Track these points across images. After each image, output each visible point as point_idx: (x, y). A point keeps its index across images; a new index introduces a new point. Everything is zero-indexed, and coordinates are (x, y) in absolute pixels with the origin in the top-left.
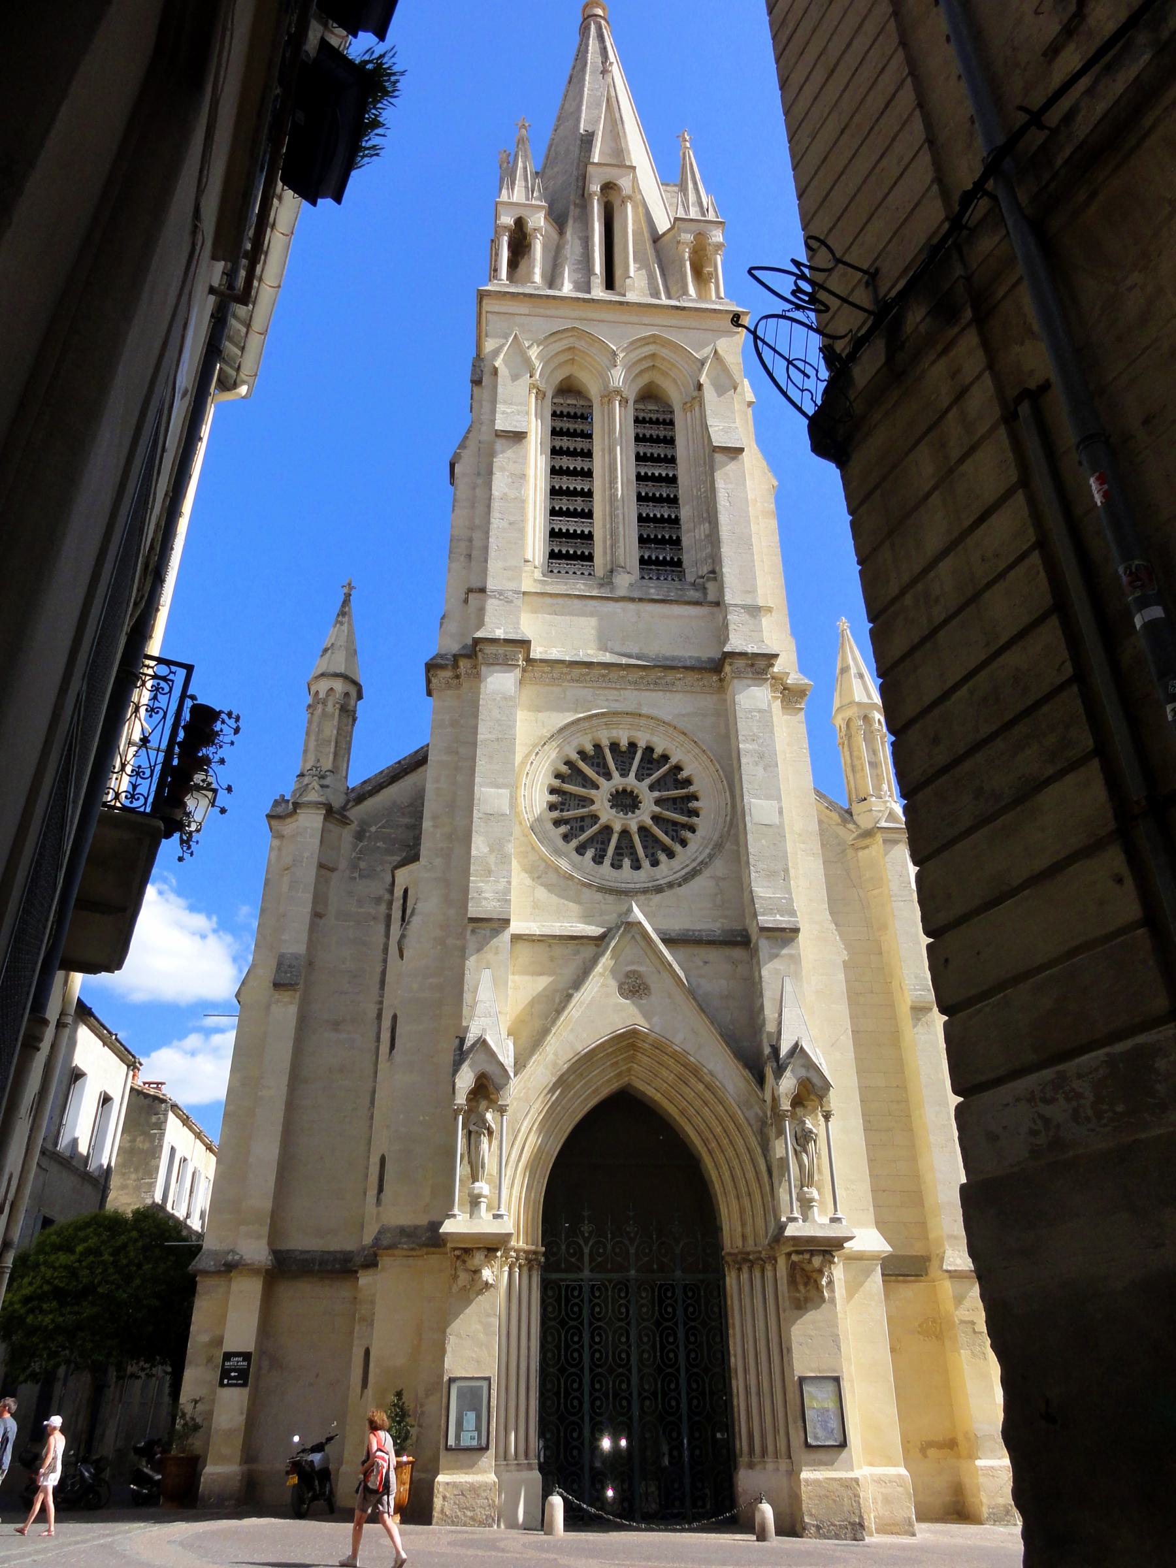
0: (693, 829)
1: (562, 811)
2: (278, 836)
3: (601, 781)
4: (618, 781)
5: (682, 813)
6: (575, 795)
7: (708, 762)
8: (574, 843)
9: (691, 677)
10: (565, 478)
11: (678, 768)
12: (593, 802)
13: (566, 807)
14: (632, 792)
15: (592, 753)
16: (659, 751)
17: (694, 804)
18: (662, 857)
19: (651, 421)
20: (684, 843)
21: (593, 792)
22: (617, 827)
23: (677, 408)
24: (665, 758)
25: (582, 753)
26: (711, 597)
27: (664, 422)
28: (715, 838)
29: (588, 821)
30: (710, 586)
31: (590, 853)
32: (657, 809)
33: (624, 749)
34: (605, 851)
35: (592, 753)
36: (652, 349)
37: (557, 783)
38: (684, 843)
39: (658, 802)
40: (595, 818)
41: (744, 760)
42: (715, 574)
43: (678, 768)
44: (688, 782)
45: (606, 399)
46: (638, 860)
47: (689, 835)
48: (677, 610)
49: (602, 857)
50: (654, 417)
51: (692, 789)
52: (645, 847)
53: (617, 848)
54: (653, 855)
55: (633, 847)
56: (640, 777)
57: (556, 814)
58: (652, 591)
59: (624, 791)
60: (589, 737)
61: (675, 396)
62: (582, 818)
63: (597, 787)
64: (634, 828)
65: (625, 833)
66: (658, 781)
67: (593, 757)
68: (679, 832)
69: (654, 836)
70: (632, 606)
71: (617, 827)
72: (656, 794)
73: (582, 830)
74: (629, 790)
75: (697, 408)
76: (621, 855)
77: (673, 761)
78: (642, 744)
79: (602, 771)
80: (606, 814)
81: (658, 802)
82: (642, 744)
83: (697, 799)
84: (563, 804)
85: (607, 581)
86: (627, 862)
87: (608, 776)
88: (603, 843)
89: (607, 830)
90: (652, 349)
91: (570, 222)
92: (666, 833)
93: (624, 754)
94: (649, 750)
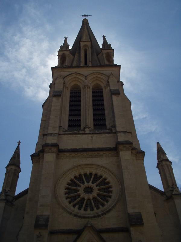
0: (110, 197)
5: (107, 193)
8: (72, 204)
9: (107, 153)
11: (105, 179)
12: (79, 191)
14: (91, 187)
16: (99, 174)
18: (101, 206)
19: (97, 92)
20: (107, 201)
21: (79, 188)
22: (86, 198)
23: (103, 88)
24: (101, 177)
26: (114, 131)
27: (100, 92)
30: (113, 129)
33: (88, 175)
34: (82, 206)
35: (78, 177)
36: (96, 75)
39: (99, 190)
40: (79, 196)
42: (114, 126)
43: (105, 179)
44: (108, 183)
47: (109, 199)
48: (103, 135)
50: (97, 91)
51: (110, 185)
52: (95, 204)
54: (98, 206)
55: (91, 204)
58: (96, 131)
59: (88, 187)
61: (102, 85)
62: (75, 196)
64: (91, 198)
68: (105, 198)
70: (90, 135)
71: (86, 198)
74: (90, 186)
77: (103, 177)
78: (94, 173)
80: (83, 194)
81: (99, 190)
82: (94, 173)
83: (111, 188)
85: (84, 130)
87: (83, 183)
90: (96, 75)
91: (76, 54)
92: (102, 199)
93: (88, 177)
94: (96, 175)
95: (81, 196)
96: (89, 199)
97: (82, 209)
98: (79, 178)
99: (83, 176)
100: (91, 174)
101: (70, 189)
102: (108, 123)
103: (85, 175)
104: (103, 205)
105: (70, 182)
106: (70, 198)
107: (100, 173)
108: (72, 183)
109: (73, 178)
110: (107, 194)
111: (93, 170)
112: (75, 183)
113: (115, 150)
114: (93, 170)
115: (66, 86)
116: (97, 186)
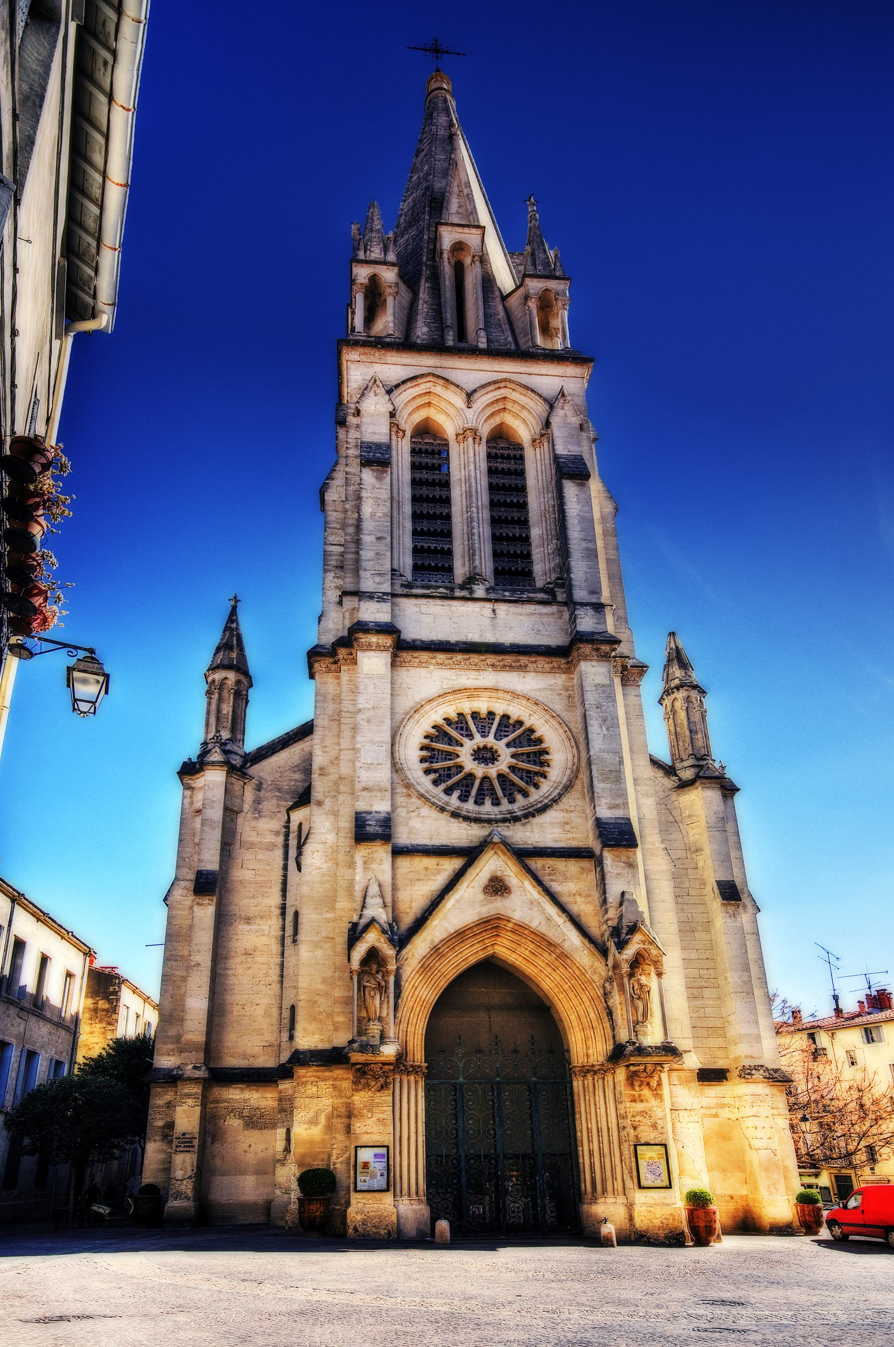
1: (431, 762)
2: (188, 787)
3: (465, 740)
4: (479, 741)
5: (535, 764)
6: (442, 751)
7: (557, 726)
12: (458, 756)
13: (435, 760)
14: (492, 748)
15: (456, 719)
17: (547, 757)
25: (447, 720)
28: (564, 782)
29: (454, 770)
31: (456, 794)
32: (514, 761)
34: (469, 792)
35: (456, 719)
37: (427, 741)
39: (514, 756)
46: (497, 799)
47: (542, 780)
49: (467, 797)
52: (503, 789)
53: (479, 789)
54: (510, 795)
55: (493, 789)
56: (498, 737)
59: (485, 748)
60: (454, 707)
62: (449, 768)
63: (462, 745)
66: (514, 740)
67: (457, 723)
68: (532, 779)
69: (510, 781)
72: (513, 750)
73: (449, 777)
76: (484, 795)
79: (464, 733)
84: (431, 757)
87: (470, 736)
88: (467, 786)
89: (471, 776)
92: (521, 779)
93: (484, 721)
97: (471, 800)
98: (460, 722)
101: (433, 750)
106: (436, 771)
108: (439, 734)
110: (536, 768)
112: (446, 734)
116: (508, 745)
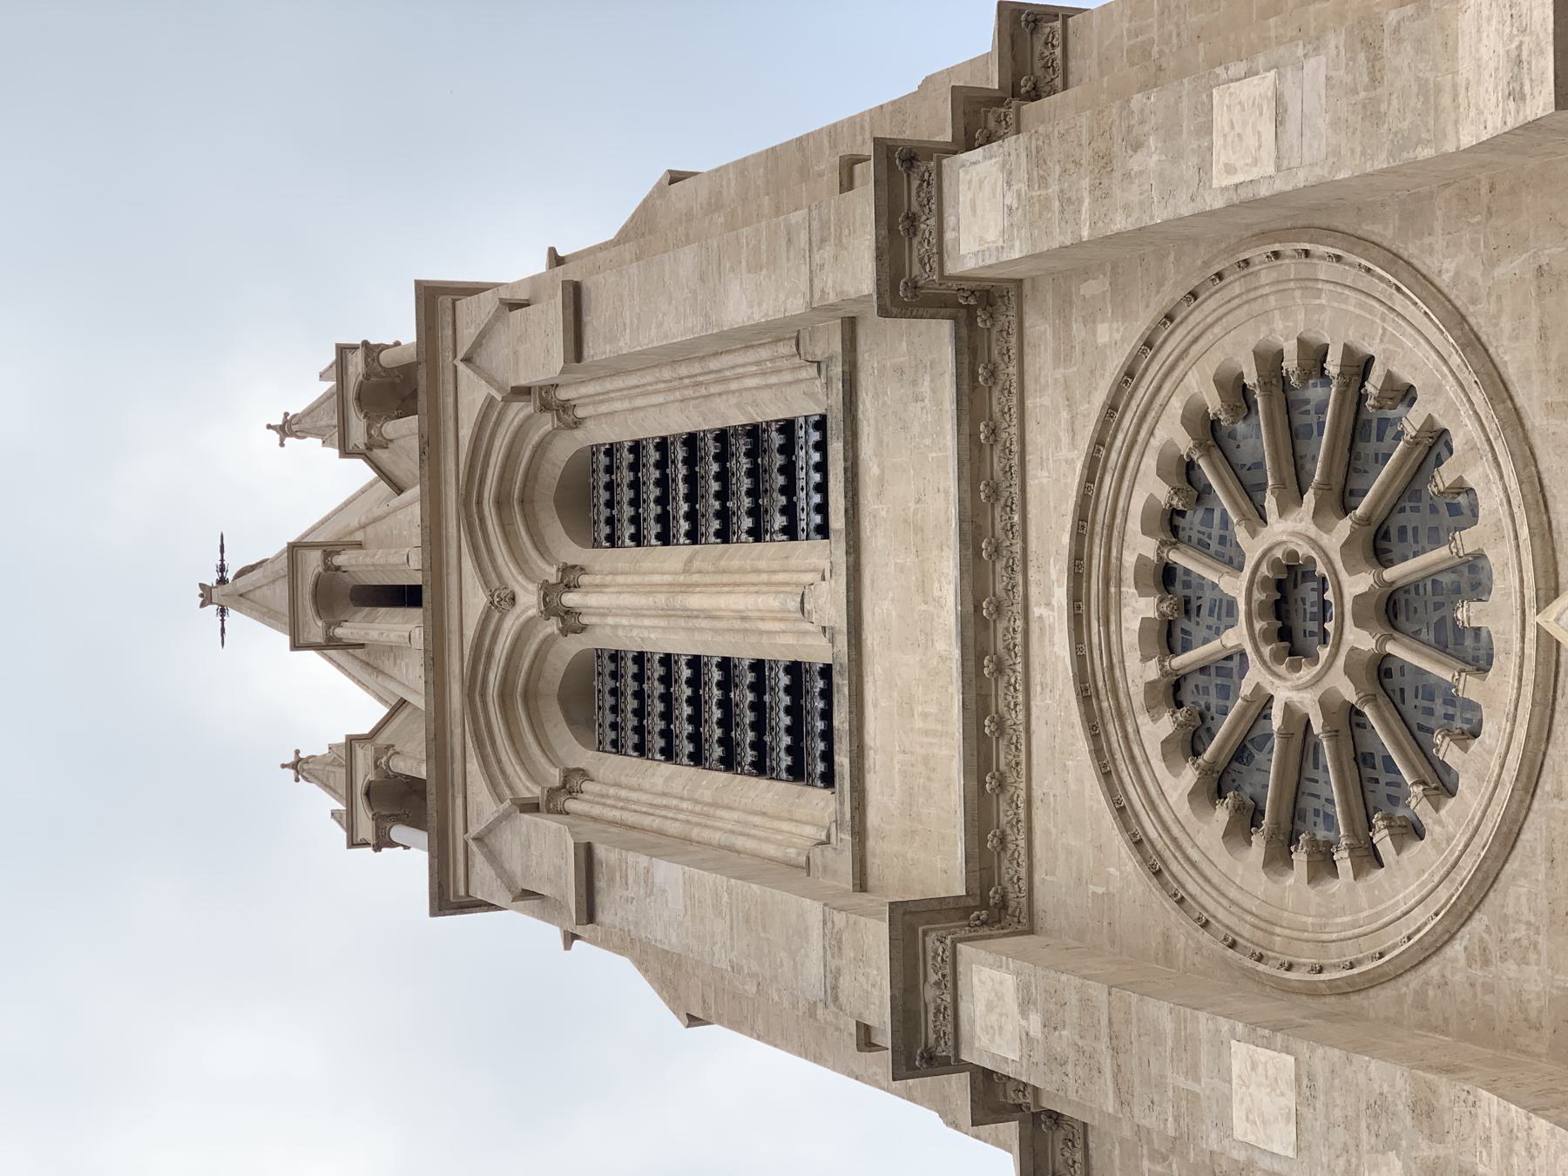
8: (1417, 803)
10: (704, 730)
22: (1360, 639)
38: (1408, 395)
41: (1120, 223)
42: (790, 334)
45: (571, 621)
47: (1373, 385)
57: (1343, 859)
60: (1144, 720)
65: (1390, 609)
71: (1360, 639)
72: (1270, 503)
75: (563, 394)
83: (1280, 355)
86: (1467, 613)
93: (1182, 610)
95: (1349, 693)
96: (1390, 609)
97: (1471, 688)
99: (1178, 661)
100: (1167, 576)
102: (788, 395)
103: (1168, 637)
104: (1436, 443)
105: (1222, 814)
107: (1151, 488)
109: (1189, 775)
111: (1130, 560)
113: (983, 314)
114: (1130, 560)
115: (552, 793)
